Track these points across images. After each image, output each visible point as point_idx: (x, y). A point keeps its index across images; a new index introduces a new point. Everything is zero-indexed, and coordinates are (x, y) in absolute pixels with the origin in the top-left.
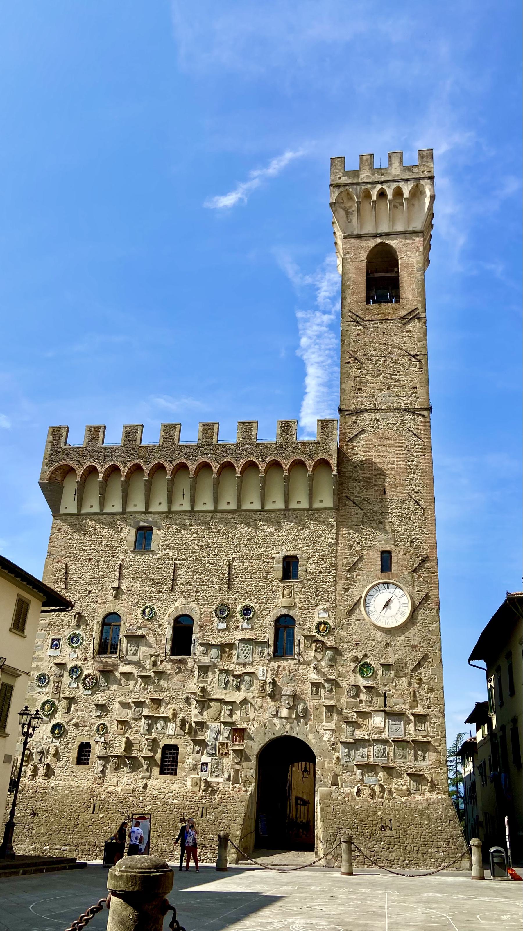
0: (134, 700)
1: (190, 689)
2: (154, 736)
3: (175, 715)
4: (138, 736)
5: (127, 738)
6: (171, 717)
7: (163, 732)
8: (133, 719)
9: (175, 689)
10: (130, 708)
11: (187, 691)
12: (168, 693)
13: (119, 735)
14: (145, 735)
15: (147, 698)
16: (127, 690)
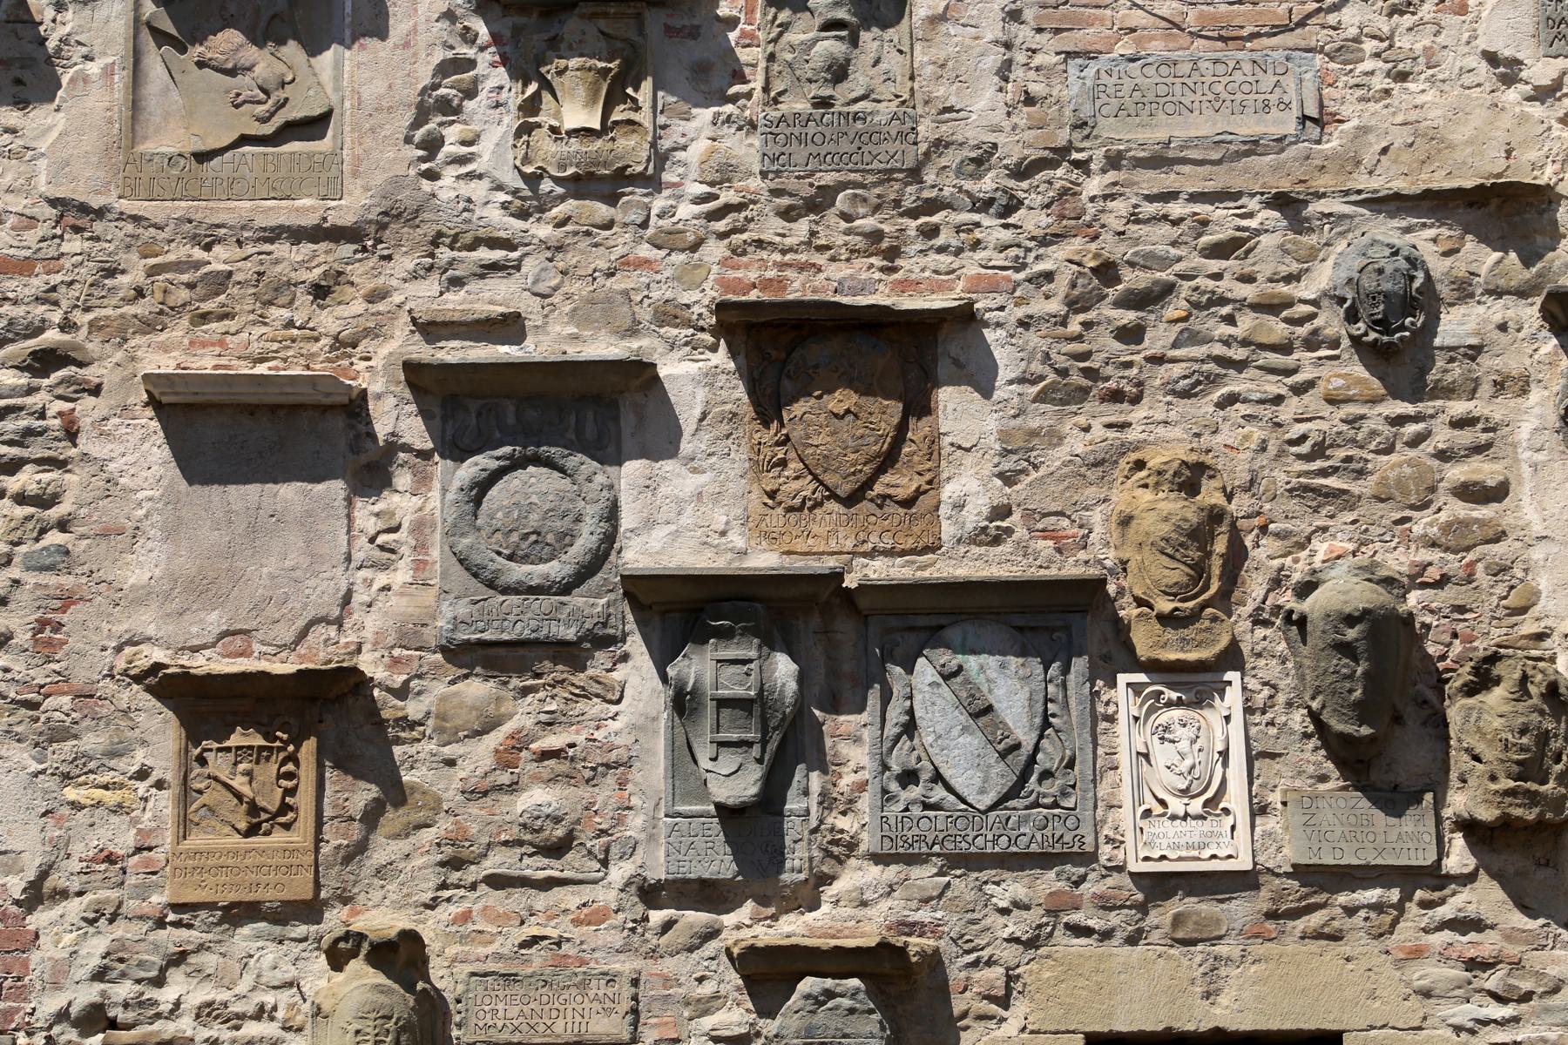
0: (454, 352)
1: (1429, 141)
2: (856, 907)
3: (1211, 554)
4: (589, 914)
5: (401, 956)
6: (1145, 581)
7: (1034, 827)
8: (469, 655)
9: (1158, 161)
10: (371, 471)
11: (1363, 182)
12: (1033, 220)
13: (238, 913)
14: (711, 895)
15: (668, 315)
16: (306, 209)
